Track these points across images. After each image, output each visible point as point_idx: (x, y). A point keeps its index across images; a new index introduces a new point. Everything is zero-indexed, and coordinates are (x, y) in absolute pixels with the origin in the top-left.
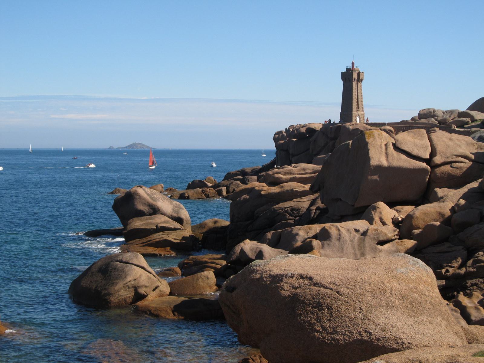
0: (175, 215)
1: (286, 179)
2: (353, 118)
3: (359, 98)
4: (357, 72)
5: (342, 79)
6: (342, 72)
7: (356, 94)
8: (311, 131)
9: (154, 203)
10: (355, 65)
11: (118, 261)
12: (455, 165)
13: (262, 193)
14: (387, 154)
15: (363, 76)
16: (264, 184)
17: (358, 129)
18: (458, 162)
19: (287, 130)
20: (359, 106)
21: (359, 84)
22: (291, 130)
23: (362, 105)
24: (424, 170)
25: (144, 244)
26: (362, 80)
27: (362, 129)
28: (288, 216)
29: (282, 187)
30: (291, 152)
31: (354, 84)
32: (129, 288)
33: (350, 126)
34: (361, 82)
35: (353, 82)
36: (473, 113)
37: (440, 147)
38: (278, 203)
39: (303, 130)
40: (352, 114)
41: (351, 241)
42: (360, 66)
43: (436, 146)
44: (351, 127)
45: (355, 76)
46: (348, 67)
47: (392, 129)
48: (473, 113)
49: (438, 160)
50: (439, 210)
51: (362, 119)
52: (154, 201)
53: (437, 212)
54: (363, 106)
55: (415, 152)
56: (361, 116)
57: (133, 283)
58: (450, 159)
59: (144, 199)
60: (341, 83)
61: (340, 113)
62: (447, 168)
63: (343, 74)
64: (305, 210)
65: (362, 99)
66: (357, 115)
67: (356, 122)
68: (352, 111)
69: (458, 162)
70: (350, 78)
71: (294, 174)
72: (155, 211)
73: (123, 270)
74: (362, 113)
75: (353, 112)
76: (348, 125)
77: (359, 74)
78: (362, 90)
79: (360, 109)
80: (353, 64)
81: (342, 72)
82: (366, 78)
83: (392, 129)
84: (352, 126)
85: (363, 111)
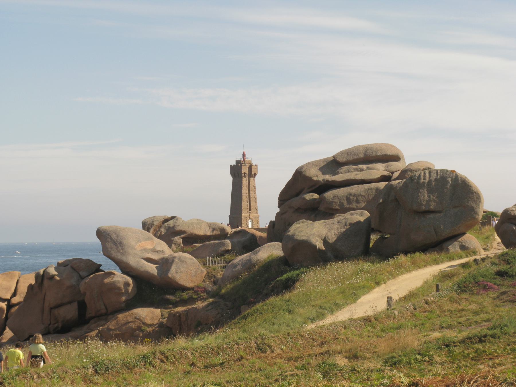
2: (243, 222)
4: (248, 165)
5: (231, 173)
6: (231, 166)
10: (247, 156)
15: (257, 169)
21: (251, 179)
26: (255, 175)
31: (245, 181)
34: (254, 177)
35: (243, 178)
40: (241, 218)
42: (253, 158)
45: (245, 170)
46: (239, 159)
51: (255, 223)
54: (256, 206)
56: (254, 219)
60: (230, 179)
63: (232, 168)
65: (255, 198)
67: (248, 226)
74: (256, 215)
77: (250, 168)
79: (252, 210)
80: (244, 155)
81: (231, 166)
85: (257, 213)
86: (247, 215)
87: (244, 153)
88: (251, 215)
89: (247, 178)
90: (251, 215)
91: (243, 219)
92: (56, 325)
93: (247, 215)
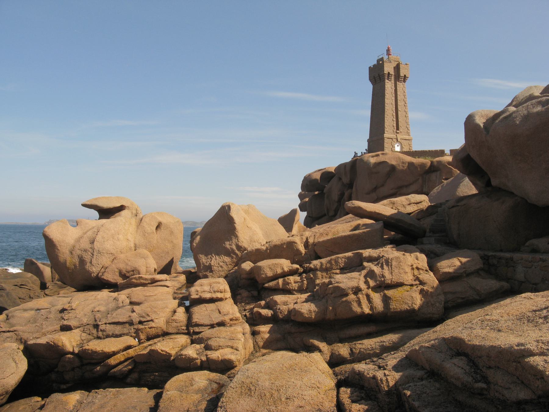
2: (386, 145)
3: (399, 109)
4: (394, 64)
7: (394, 103)
17: (383, 163)
20: (400, 124)
21: (400, 85)
23: (407, 123)
27: (394, 163)
31: (389, 85)
34: (404, 81)
35: (387, 81)
39: (318, 176)
40: (383, 139)
45: (389, 68)
60: (370, 87)
61: (368, 141)
66: (395, 140)
68: (384, 133)
75: (386, 135)
77: (397, 68)
78: (407, 96)
79: (401, 129)
84: (375, 158)
85: (408, 134)
86: (393, 136)
87: (388, 48)
88: (399, 137)
89: (393, 82)
90: (399, 137)
91: (386, 141)
93: (393, 136)
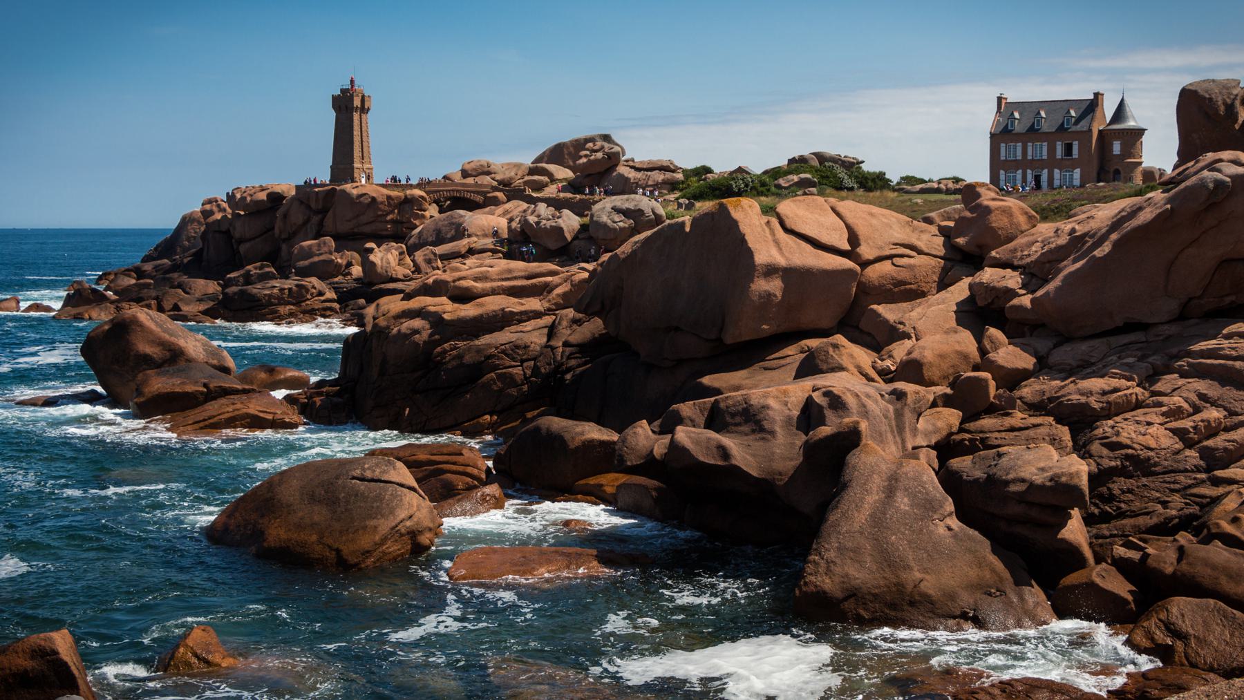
0: (215, 362)
1: (483, 290)
8: (276, 199)
9: (173, 339)
10: (356, 83)
11: (354, 478)
12: (896, 260)
13: (446, 316)
14: (777, 243)
16: (444, 299)
18: (902, 256)
19: (230, 197)
22: (238, 196)
24: (850, 272)
25: (201, 424)
28: (508, 362)
29: (482, 305)
30: (237, 235)
31: (356, 116)
32: (402, 535)
33: (359, 187)
36: (552, 167)
37: (862, 231)
38: (477, 337)
39: (263, 196)
41: (886, 417)
42: (365, 86)
43: (856, 228)
44: (355, 192)
47: (423, 194)
48: (552, 167)
49: (866, 251)
50: (958, 348)
52: (171, 335)
53: (957, 352)
55: (825, 239)
57: (408, 523)
58: (888, 252)
59: (151, 332)
62: (886, 267)
63: (335, 99)
64: (538, 348)
69: (902, 256)
70: (347, 107)
71: (492, 280)
72: (174, 357)
73: (379, 498)
75: (356, 165)
76: (348, 187)
77: (363, 101)
80: (352, 82)
82: (373, 104)
83: (423, 194)
92: (1233, 298)
